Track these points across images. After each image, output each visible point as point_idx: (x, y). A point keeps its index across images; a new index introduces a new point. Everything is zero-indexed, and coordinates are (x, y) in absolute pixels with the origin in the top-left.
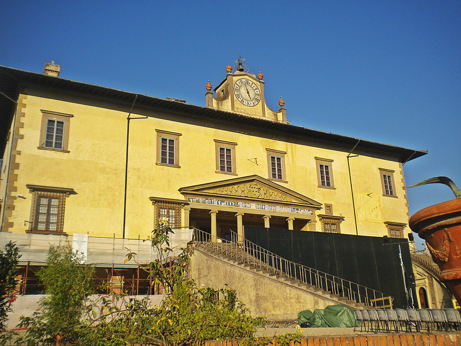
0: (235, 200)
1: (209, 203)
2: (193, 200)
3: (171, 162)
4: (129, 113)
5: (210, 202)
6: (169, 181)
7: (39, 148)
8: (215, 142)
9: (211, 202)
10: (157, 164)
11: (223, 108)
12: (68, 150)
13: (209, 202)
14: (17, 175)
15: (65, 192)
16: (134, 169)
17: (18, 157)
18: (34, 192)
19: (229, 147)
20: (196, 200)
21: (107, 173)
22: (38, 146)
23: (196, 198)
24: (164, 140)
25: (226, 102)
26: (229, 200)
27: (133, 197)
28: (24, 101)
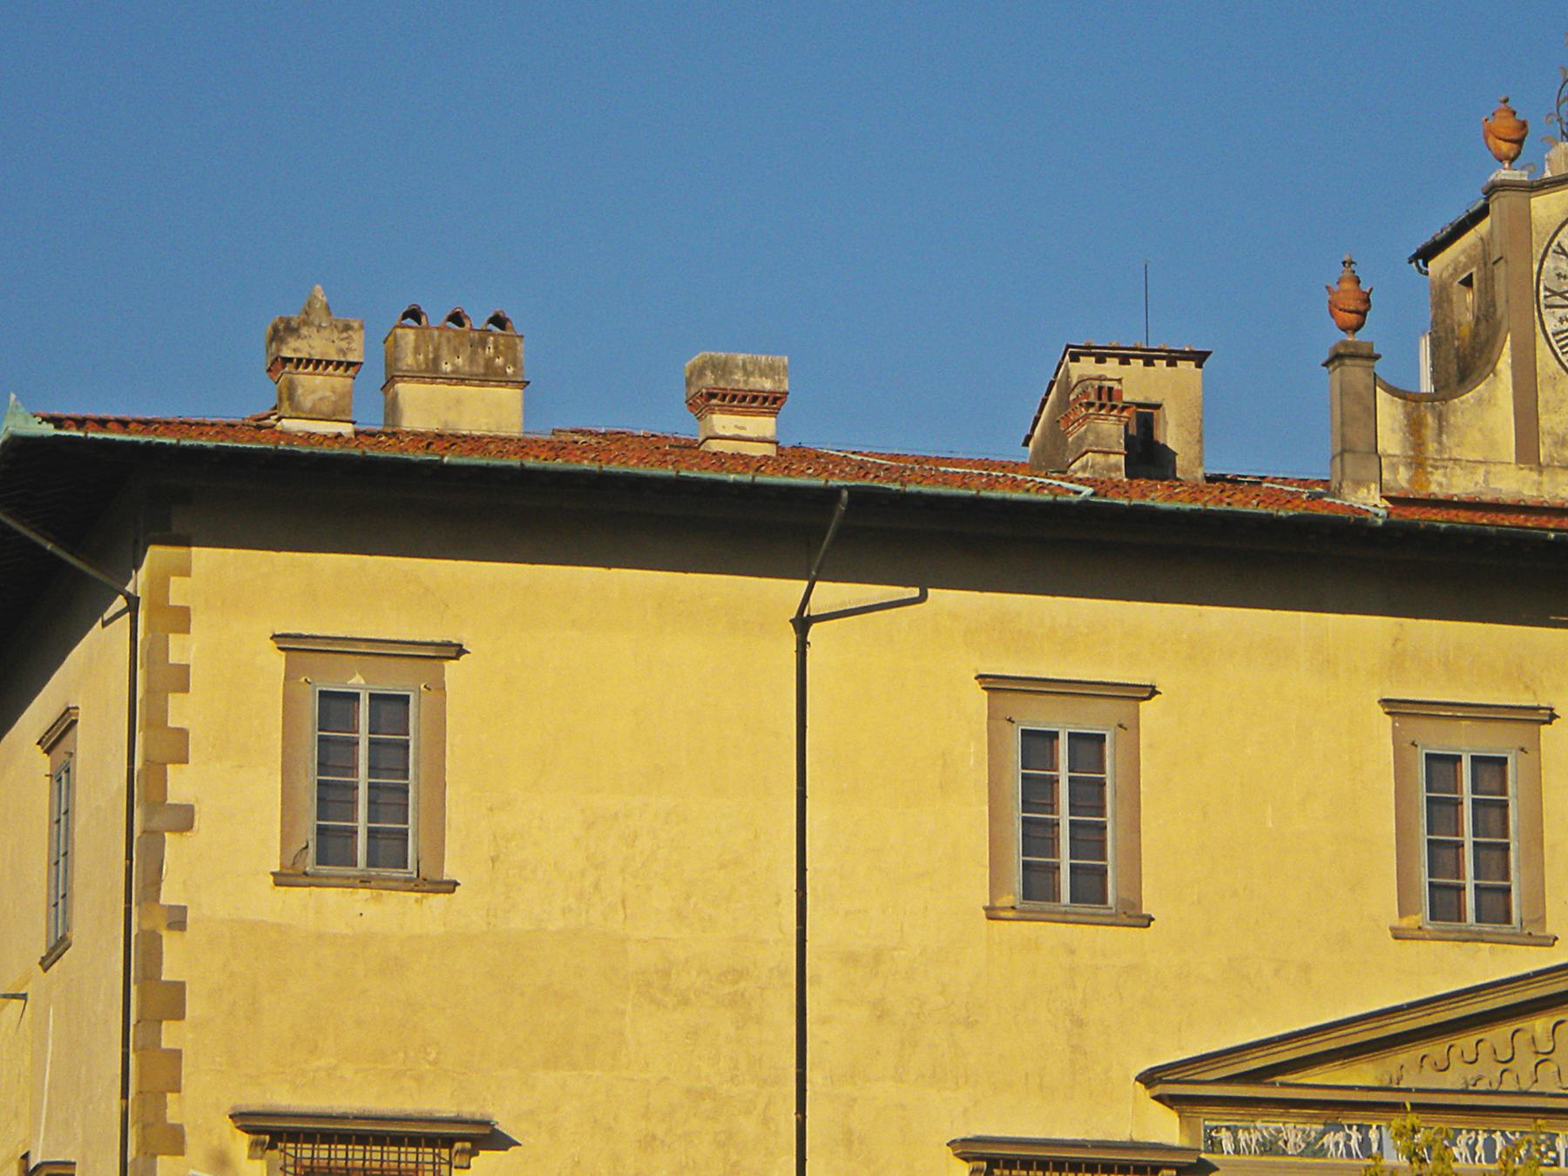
0: (1526, 1124)
1: (1349, 1154)
2: (1236, 1141)
3: (1089, 886)
4: (806, 583)
5: (1354, 1144)
6: (1080, 1023)
7: (282, 879)
8: (1389, 718)
9: (1365, 1144)
10: (992, 913)
11: (1455, 454)
12: (449, 873)
13: (1347, 1147)
14: (176, 1055)
15: (448, 1141)
16: (851, 958)
17: (171, 943)
18: (276, 1147)
19: (1489, 740)
20: (1255, 1136)
21: (685, 1002)
22: (277, 869)
23: (1259, 1124)
24: (1037, 743)
25: (1480, 401)
26: (1495, 1121)
27: (849, 1143)
28: (179, 588)
